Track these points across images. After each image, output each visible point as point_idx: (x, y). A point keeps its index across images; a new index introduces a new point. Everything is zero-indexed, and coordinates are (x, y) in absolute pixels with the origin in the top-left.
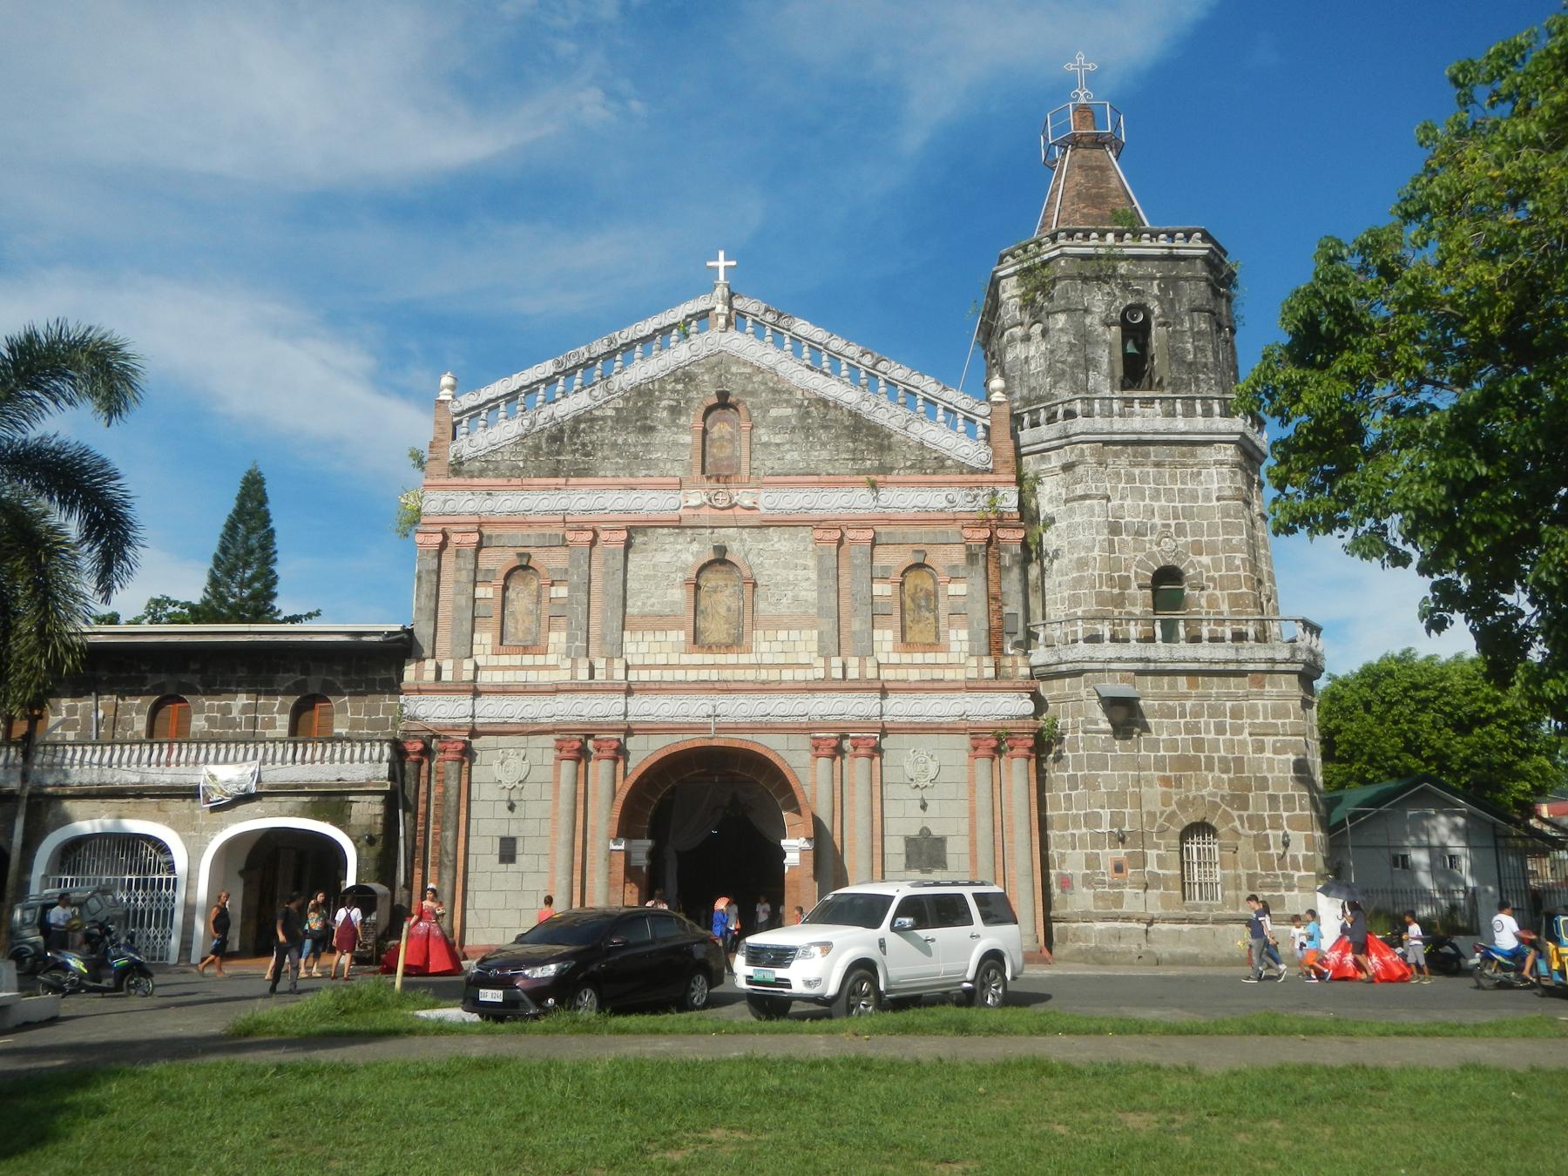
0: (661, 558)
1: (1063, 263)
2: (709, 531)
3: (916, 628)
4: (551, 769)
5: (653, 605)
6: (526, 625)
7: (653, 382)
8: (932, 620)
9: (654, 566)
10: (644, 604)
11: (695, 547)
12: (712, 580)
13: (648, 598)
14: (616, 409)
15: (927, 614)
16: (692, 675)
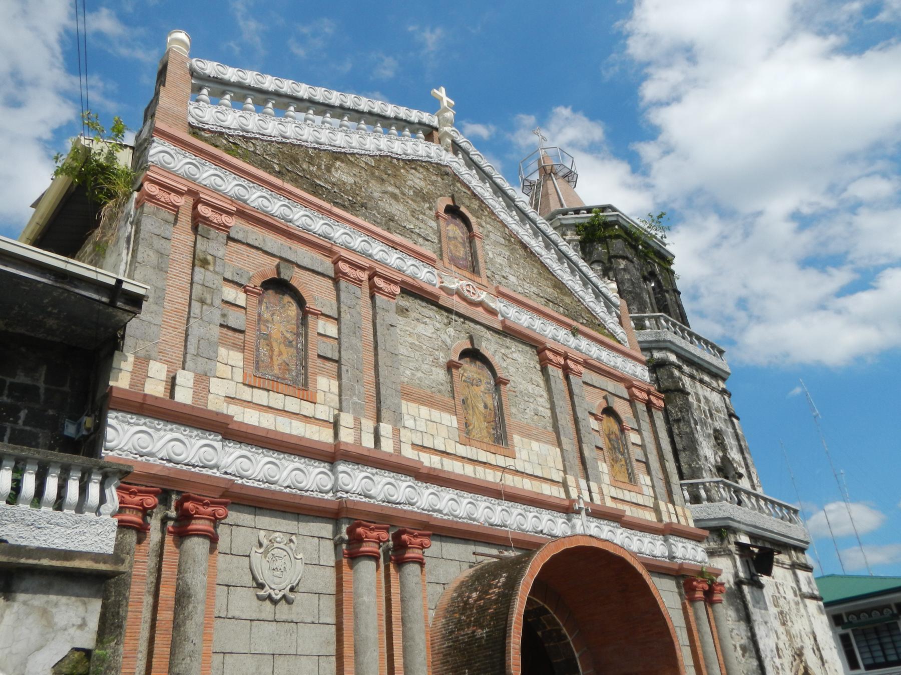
0: (420, 328)
1: (617, 227)
2: (462, 320)
3: (617, 467)
4: (331, 574)
5: (420, 379)
6: (285, 357)
7: (398, 159)
8: (623, 462)
9: (419, 336)
10: (413, 374)
11: (451, 330)
12: (471, 369)
13: (417, 370)
14: (366, 163)
15: (620, 456)
16: (468, 471)
